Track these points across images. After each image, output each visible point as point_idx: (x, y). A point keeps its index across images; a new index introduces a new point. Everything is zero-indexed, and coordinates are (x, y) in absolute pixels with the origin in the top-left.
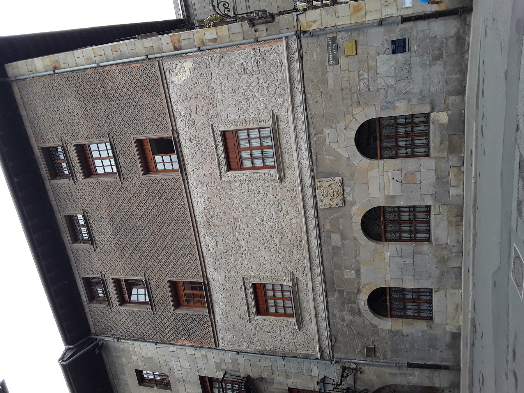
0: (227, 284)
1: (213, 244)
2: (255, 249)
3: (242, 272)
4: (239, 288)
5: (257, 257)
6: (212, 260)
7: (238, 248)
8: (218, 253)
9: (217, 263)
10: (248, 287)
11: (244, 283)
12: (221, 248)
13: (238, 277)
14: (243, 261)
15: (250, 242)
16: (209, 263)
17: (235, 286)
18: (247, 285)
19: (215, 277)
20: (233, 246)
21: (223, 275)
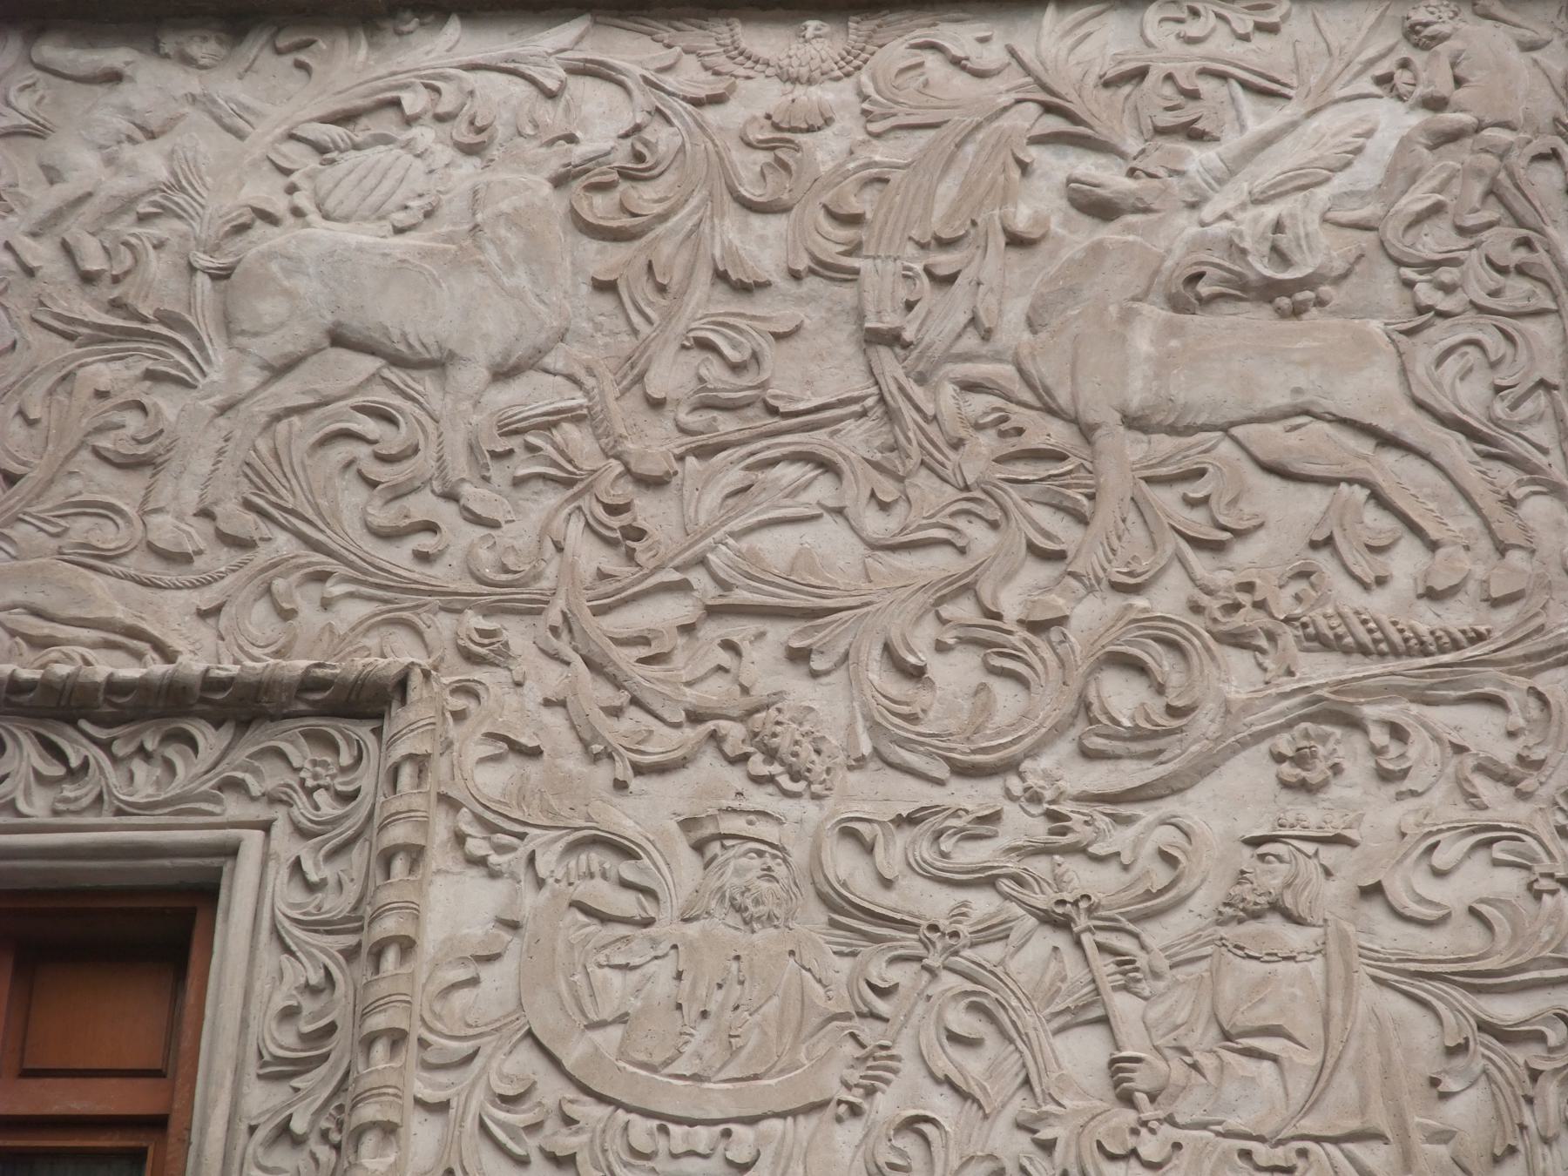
0: (223, 369)
1: (1220, 200)
2: (1083, 1054)
3: (511, 703)
4: (109, 597)
5: (876, 1067)
6: (825, 151)
7: (1123, 697)
8: (1006, 290)
9: (762, 246)
10: (145, 782)
11: (243, 705)
12: (1141, 358)
13: (399, 603)
14: (774, 760)
15: (1285, 980)
16: (760, 98)
17: (164, 530)
18: (188, 771)
19: (415, 164)
20: (1167, 599)
21: (470, 313)
